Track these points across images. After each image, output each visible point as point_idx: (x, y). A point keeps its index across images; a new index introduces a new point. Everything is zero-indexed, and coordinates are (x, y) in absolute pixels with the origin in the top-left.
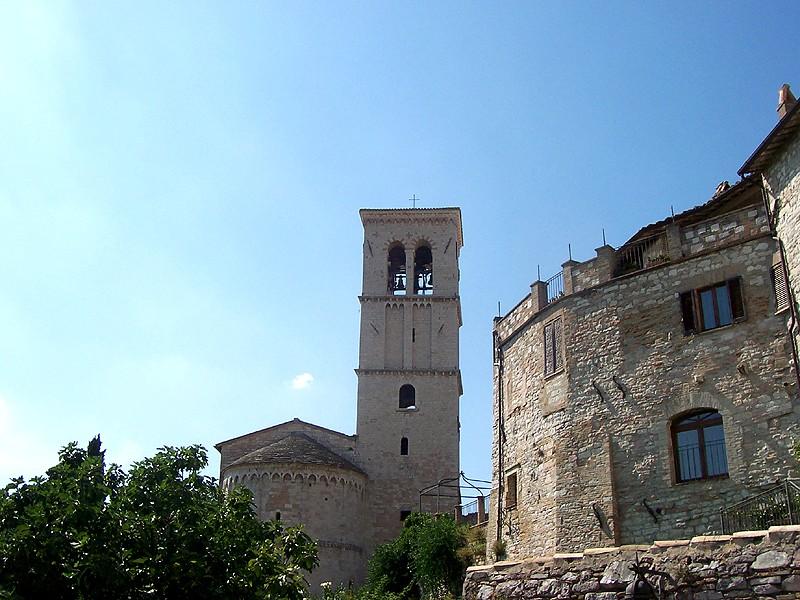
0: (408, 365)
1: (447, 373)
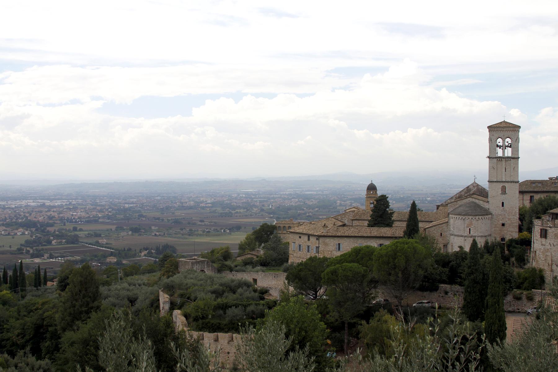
0: (504, 180)
1: (516, 182)
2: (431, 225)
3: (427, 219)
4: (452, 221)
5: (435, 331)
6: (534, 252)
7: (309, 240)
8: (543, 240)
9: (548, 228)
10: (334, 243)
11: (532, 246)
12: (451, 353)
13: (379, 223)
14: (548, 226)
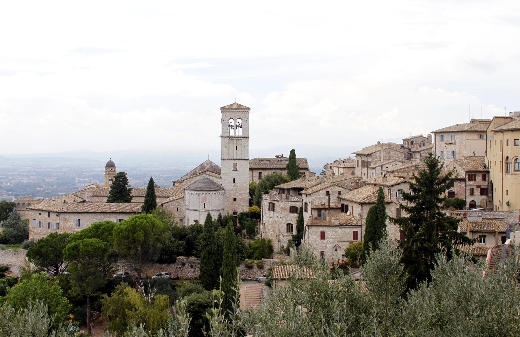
2: (168, 200)
3: (164, 195)
4: (187, 197)
5: (220, 303)
6: (263, 224)
7: (49, 216)
8: (272, 213)
9: (276, 202)
10: (74, 219)
11: (261, 218)
12: (234, 324)
13: (118, 199)
14: (276, 200)
